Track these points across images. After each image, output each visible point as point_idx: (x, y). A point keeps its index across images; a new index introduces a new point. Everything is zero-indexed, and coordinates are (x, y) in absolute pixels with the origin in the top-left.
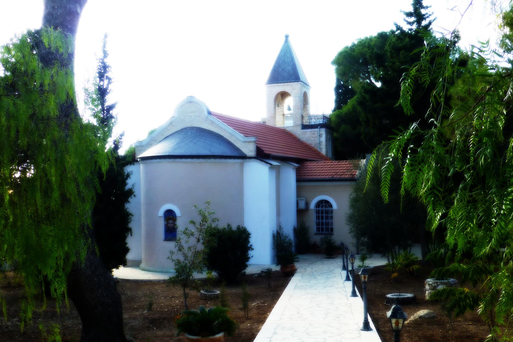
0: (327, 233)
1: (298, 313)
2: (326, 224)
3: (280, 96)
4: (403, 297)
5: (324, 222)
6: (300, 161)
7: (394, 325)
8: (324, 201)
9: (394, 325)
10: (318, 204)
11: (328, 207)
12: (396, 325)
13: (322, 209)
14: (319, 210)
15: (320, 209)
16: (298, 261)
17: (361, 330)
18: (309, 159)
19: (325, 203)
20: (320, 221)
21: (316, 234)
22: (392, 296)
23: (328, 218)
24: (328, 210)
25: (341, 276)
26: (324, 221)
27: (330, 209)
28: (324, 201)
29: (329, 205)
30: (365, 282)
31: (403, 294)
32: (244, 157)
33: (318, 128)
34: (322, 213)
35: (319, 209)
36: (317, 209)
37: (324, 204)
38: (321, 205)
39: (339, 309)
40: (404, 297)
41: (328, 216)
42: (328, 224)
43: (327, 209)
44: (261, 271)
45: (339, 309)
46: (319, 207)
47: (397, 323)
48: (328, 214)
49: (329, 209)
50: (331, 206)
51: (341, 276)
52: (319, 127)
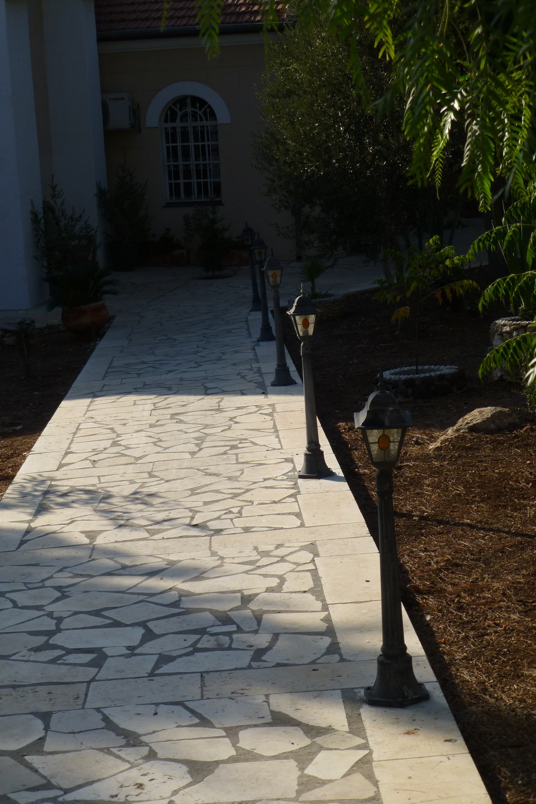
0: (203, 200)
1: (115, 444)
4: (427, 375)
5: (193, 168)
7: (375, 448)
8: (188, 101)
9: (375, 448)
10: (171, 109)
11: (201, 120)
12: (380, 448)
13: (184, 124)
14: (174, 128)
15: (178, 124)
16: (114, 293)
17: (301, 477)
19: (194, 105)
20: (181, 162)
21: (169, 205)
22: (396, 374)
23: (204, 154)
24: (202, 127)
25: (248, 329)
26: (192, 162)
28: (188, 101)
29: (205, 113)
30: (306, 336)
31: (426, 367)
34: (185, 137)
35: (174, 125)
36: (170, 125)
38: (180, 114)
39: (236, 423)
40: (430, 377)
41: (203, 146)
42: (205, 171)
43: (199, 124)
45: (236, 423)
46: (173, 120)
47: (384, 441)
48: (203, 140)
49: (205, 123)
50: (212, 115)
51: (248, 329)
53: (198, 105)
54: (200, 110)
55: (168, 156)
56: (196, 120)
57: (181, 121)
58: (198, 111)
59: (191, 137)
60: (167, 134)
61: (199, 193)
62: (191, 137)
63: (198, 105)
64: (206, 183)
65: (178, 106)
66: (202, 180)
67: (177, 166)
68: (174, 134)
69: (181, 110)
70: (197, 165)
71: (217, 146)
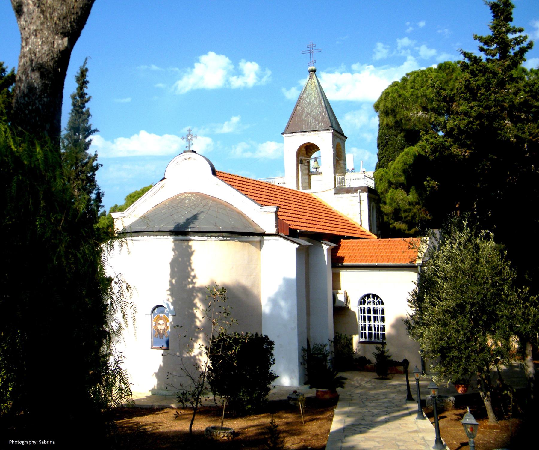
0: (377, 340)
2: (375, 328)
3: (303, 149)
5: (372, 326)
6: (336, 239)
8: (371, 296)
11: (377, 304)
15: (366, 306)
18: (346, 235)
23: (378, 320)
26: (372, 323)
27: (380, 307)
28: (371, 296)
29: (379, 302)
32: (262, 234)
33: (357, 193)
34: (369, 312)
35: (364, 306)
37: (371, 299)
38: (367, 301)
41: (378, 317)
42: (378, 328)
43: (375, 306)
44: (289, 397)
46: (364, 303)
48: (377, 314)
50: (382, 303)
52: (359, 191)
53: (375, 298)
54: (376, 300)
55: (362, 320)
56: (375, 304)
57: (368, 304)
58: (375, 300)
59: (372, 312)
60: (361, 310)
61: (375, 338)
62: (372, 312)
63: (375, 298)
64: (378, 334)
65: (366, 298)
66: (376, 332)
67: (365, 325)
68: (364, 310)
69: (368, 299)
70: (374, 325)
71: (384, 317)
